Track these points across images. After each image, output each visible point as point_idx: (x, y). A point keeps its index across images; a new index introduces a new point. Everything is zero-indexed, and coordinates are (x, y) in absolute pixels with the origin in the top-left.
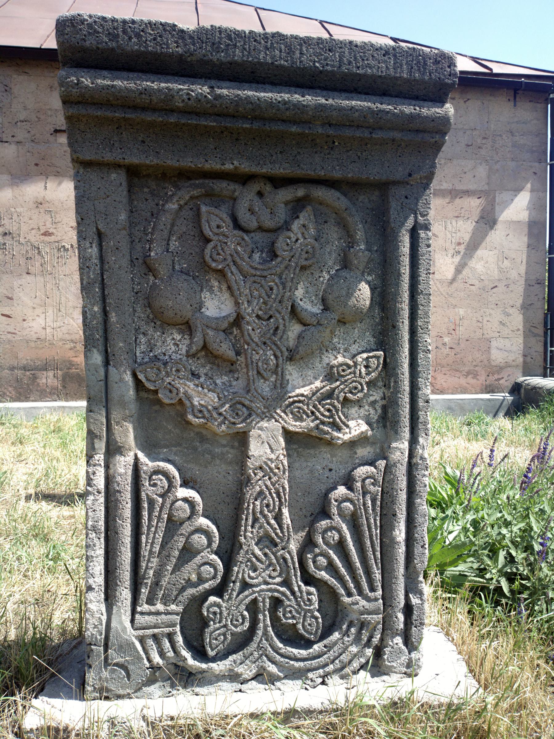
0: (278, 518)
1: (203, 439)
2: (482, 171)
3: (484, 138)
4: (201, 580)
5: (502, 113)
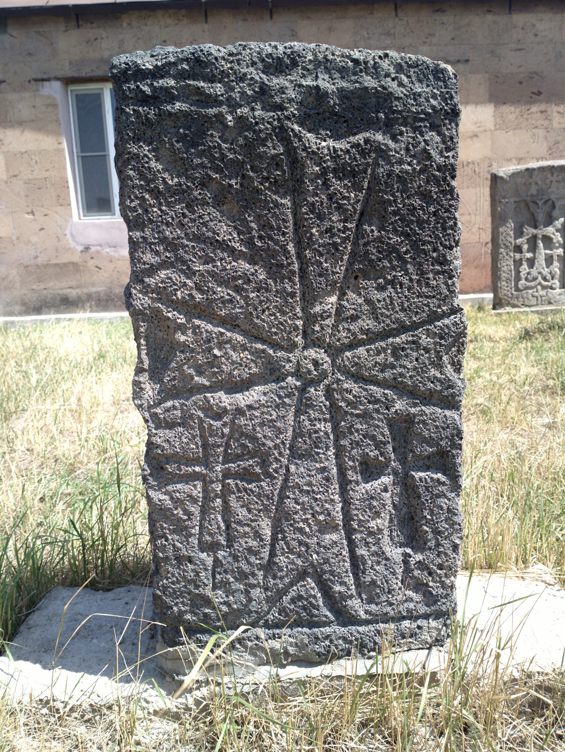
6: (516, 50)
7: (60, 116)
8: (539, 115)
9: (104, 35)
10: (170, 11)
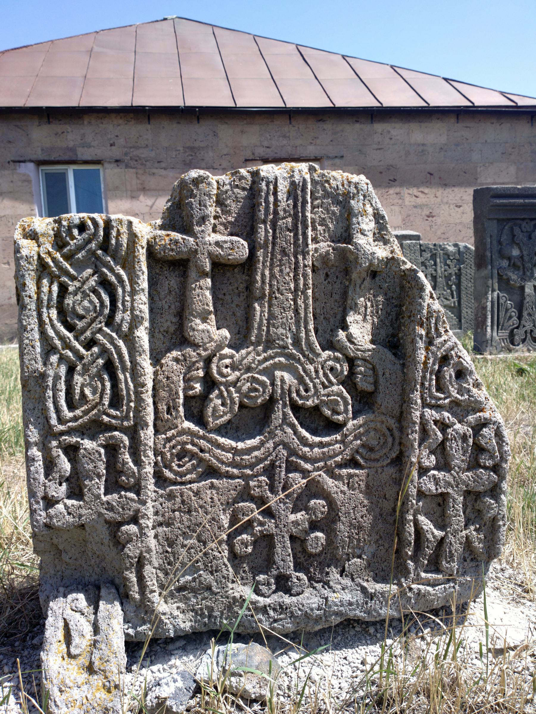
0: (532, 308)
1: (512, 289)
2: (512, 169)
3: (513, 148)
4: (513, 324)
5: (524, 130)
6: (377, 149)
7: (33, 189)
8: (395, 195)
9: (70, 130)
10: (121, 114)
